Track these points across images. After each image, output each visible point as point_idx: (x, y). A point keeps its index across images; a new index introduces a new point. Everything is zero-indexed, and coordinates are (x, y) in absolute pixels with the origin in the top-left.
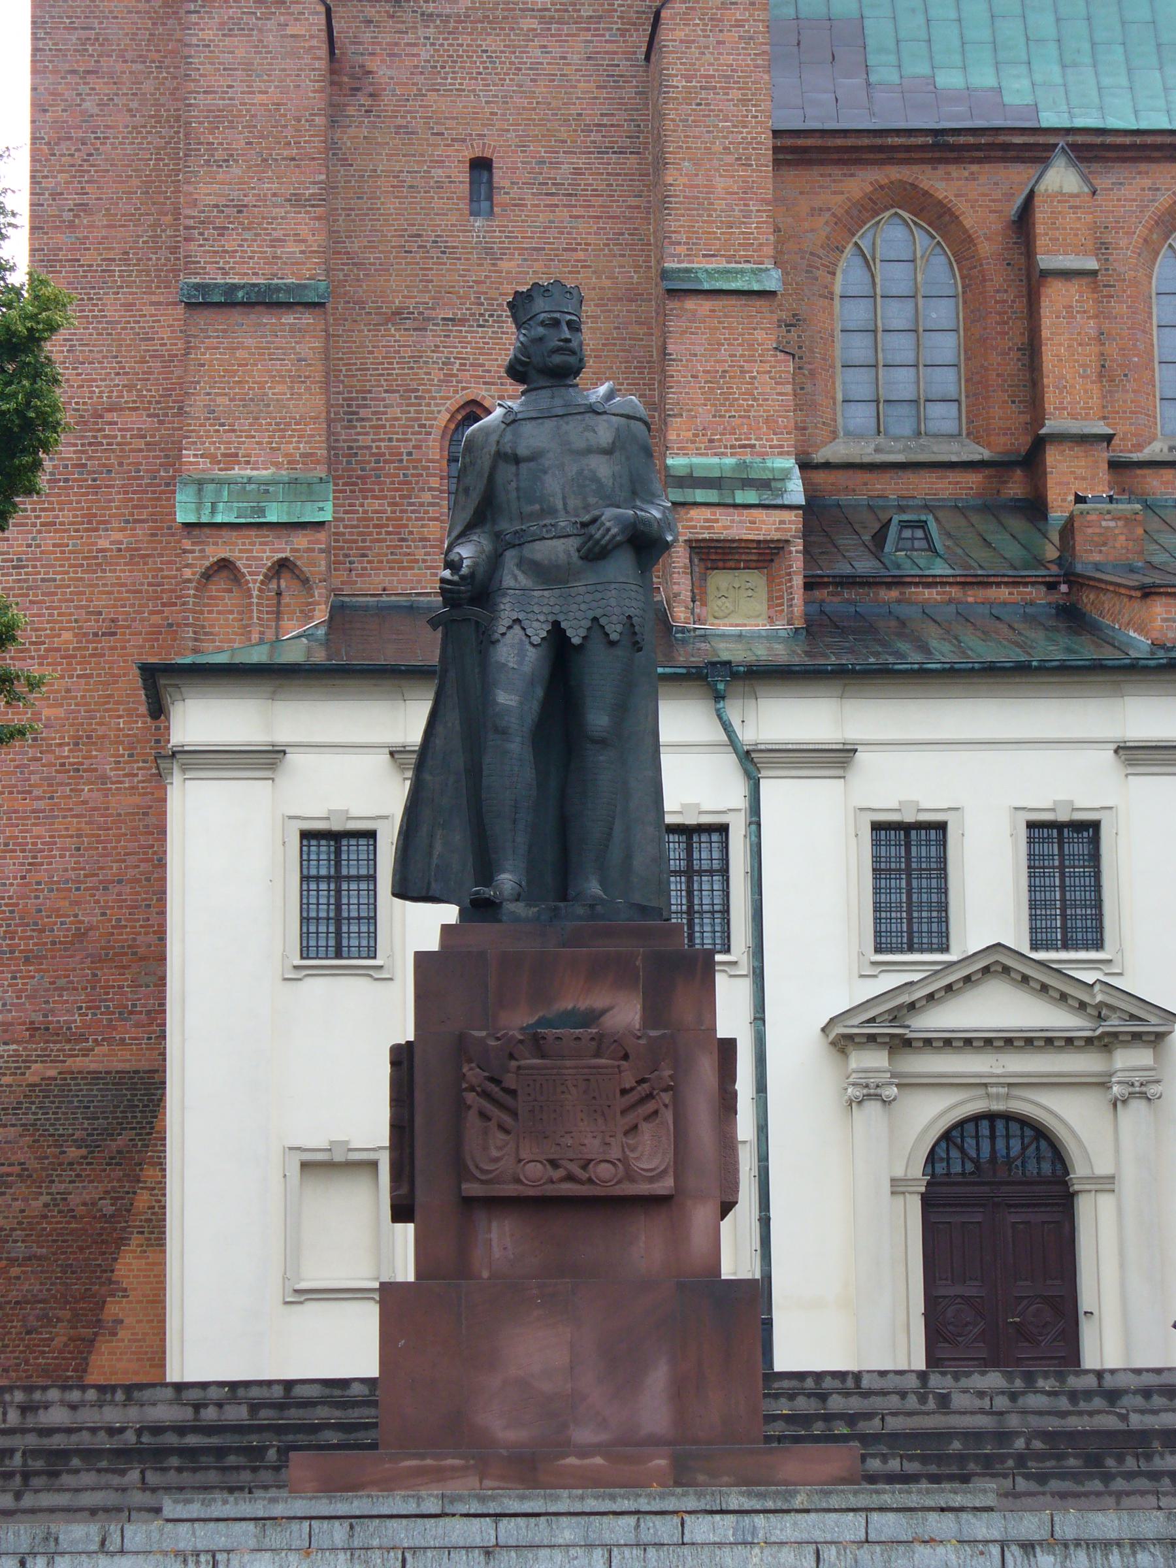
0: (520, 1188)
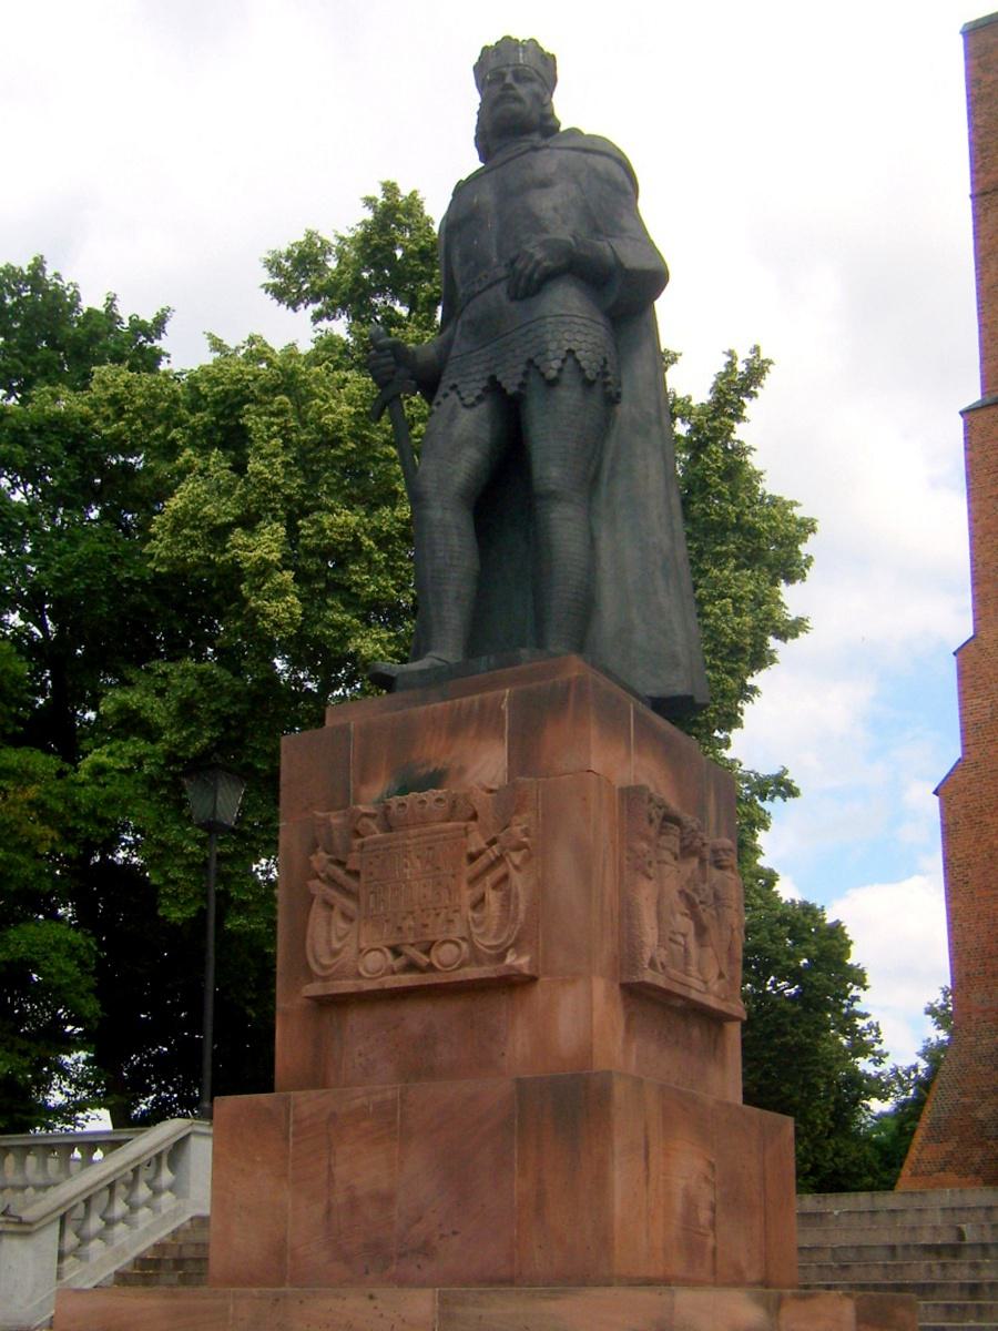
0: (360, 982)
